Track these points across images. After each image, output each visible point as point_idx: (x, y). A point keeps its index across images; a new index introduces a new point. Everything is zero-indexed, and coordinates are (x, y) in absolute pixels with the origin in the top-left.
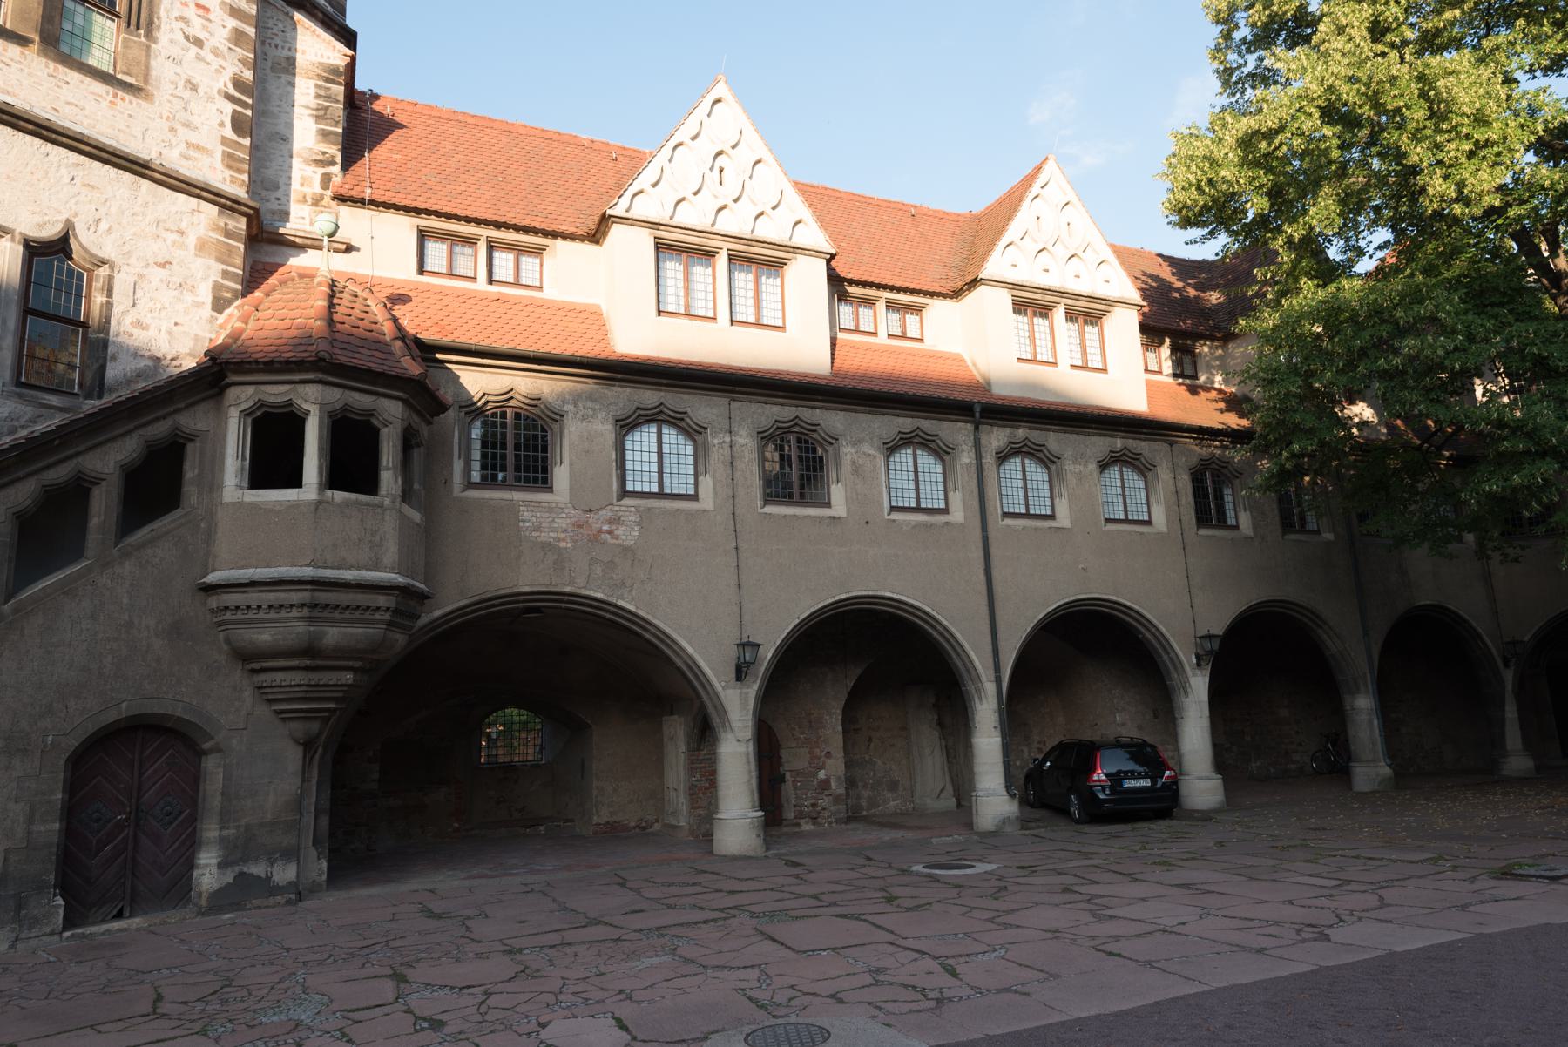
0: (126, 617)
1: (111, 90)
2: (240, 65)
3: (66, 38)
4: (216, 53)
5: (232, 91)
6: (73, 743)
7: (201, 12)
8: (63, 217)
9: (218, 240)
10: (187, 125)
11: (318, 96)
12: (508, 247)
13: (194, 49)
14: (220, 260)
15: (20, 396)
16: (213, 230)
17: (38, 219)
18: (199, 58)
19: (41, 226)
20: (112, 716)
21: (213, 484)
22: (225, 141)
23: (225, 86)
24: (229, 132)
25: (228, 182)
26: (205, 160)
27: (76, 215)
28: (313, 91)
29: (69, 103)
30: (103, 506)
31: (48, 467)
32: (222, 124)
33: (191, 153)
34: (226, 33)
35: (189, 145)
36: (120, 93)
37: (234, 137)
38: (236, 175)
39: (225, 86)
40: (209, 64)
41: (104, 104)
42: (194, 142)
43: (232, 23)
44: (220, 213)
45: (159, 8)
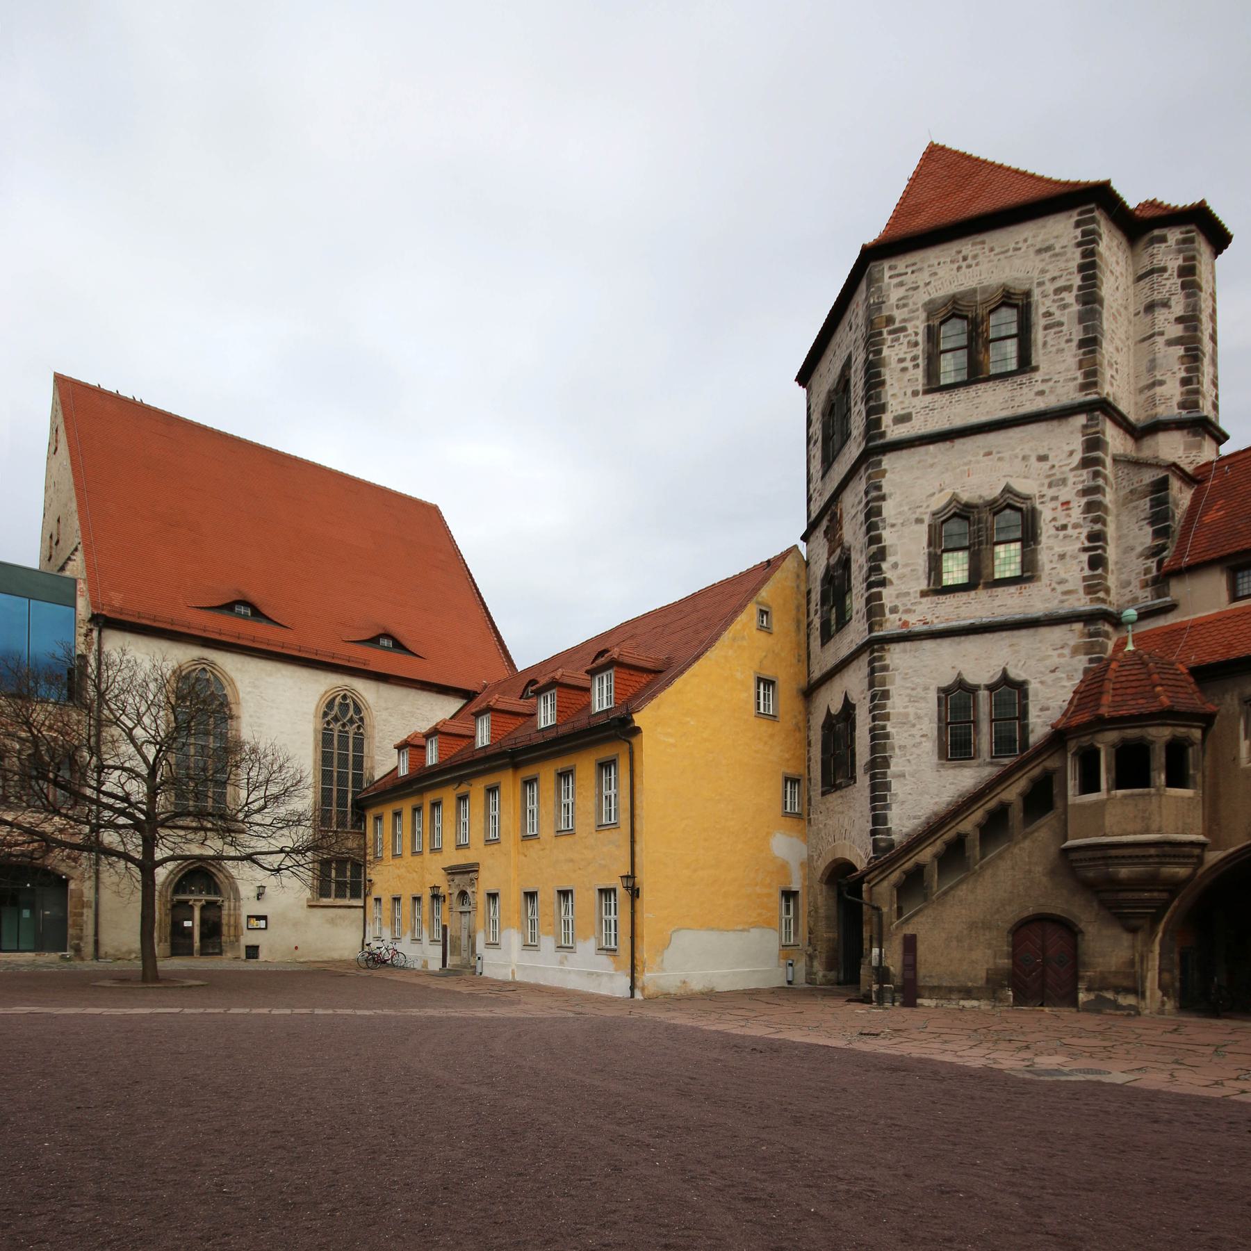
0: (1028, 867)
1: (1019, 586)
2: (1092, 524)
3: (996, 569)
4: (1075, 526)
5: (1087, 544)
6: (1008, 926)
7: (1065, 507)
8: (1001, 668)
9: (1085, 642)
10: (1059, 583)
13: (1062, 533)
14: (1086, 654)
15: (991, 764)
16: (1081, 637)
17: (991, 673)
18: (1065, 537)
19: (992, 677)
20: (1026, 914)
22: (1085, 579)
23: (1083, 544)
24: (1087, 572)
25: (1088, 603)
26: (1075, 596)
27: (1007, 664)
29: (999, 606)
30: (1016, 814)
31: (986, 802)
32: (1082, 570)
33: (1065, 597)
34: (1080, 510)
36: (1023, 586)
37: (1091, 573)
38: (1094, 596)
39: (1083, 544)
40: (1071, 536)
41: (1016, 596)
42: (1066, 589)
43: (1084, 500)
44: (1085, 626)
45: (1040, 521)
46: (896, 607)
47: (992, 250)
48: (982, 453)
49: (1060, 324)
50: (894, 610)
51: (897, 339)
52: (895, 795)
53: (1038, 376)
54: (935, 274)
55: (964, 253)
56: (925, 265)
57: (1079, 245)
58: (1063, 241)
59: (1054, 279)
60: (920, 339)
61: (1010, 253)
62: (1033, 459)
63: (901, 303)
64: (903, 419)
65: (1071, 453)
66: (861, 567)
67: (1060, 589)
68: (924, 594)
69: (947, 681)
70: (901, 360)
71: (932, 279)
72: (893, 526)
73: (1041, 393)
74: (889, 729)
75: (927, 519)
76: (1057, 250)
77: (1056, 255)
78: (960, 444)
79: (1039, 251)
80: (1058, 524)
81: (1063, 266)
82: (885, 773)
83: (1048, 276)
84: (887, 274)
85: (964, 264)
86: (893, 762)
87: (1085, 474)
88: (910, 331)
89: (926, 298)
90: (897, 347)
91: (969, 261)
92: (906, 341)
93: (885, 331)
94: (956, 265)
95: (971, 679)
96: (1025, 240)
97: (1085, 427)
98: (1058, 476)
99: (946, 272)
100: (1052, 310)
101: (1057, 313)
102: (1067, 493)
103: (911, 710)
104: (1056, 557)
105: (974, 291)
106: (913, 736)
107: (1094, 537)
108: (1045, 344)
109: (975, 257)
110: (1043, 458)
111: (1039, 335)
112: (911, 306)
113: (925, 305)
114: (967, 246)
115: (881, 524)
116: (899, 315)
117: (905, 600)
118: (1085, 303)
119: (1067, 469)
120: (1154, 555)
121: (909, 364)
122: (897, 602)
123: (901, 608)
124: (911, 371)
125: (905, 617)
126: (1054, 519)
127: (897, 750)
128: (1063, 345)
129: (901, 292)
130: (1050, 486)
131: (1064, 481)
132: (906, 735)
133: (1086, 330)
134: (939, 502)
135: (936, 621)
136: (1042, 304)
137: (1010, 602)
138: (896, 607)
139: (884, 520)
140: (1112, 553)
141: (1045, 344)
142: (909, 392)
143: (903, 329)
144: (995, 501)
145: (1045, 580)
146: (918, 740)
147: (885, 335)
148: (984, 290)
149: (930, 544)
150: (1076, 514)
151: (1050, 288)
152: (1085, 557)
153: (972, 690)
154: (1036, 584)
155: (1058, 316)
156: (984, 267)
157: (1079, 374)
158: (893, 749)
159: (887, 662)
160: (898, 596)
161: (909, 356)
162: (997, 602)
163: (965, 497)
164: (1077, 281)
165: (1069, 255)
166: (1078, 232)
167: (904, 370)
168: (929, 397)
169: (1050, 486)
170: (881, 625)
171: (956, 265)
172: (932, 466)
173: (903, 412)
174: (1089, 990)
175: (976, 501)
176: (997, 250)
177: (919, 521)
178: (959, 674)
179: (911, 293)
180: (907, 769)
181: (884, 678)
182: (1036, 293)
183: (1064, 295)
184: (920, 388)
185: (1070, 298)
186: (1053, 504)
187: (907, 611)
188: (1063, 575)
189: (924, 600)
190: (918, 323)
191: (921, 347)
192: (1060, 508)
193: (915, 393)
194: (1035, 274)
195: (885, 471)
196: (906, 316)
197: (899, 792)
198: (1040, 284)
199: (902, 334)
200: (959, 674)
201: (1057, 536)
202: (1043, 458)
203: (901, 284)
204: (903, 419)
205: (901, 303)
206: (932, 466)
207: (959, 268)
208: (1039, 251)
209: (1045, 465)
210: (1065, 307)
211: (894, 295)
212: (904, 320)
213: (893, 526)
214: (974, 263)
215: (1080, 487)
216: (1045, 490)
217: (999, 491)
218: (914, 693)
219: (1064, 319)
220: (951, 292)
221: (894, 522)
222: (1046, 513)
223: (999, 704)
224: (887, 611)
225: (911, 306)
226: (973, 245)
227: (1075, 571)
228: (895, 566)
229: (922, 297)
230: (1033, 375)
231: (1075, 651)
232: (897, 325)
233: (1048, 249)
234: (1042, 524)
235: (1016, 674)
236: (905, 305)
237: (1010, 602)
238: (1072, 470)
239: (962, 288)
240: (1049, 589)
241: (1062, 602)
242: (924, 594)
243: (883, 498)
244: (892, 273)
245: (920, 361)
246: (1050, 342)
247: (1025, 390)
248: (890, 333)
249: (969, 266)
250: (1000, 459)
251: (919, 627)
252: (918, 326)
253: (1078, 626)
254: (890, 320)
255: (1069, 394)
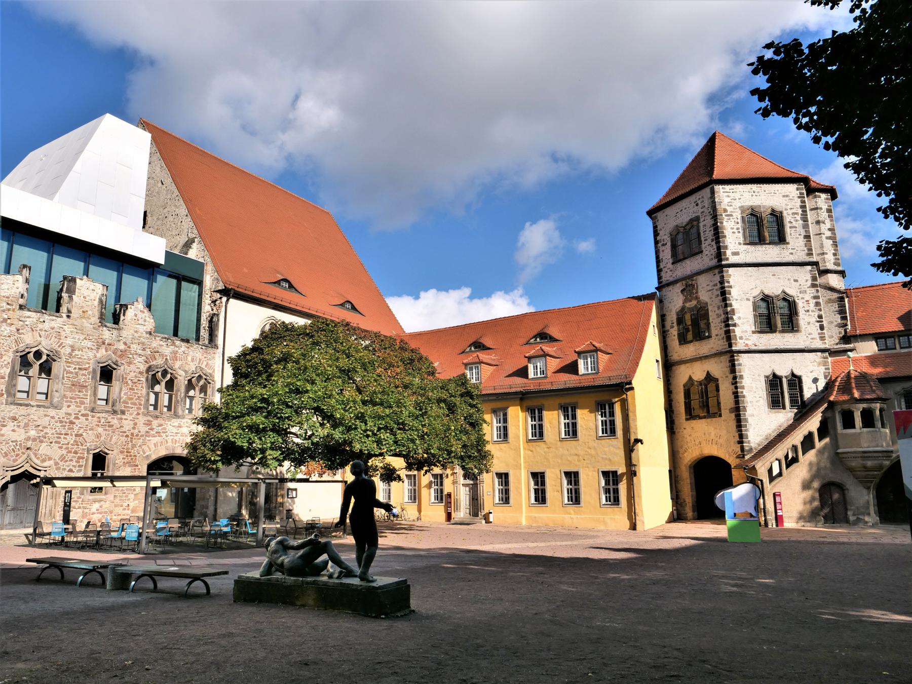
5: (818, 320)
11: (839, 307)
12: (902, 336)
13: (808, 313)
14: (824, 366)
18: (809, 315)
21: (835, 428)
22: (819, 334)
28: (837, 306)
33: (812, 341)
34: (813, 305)
35: (812, 339)
43: (815, 301)
46: (742, 337)
47: (765, 191)
48: (771, 274)
49: (796, 227)
50: (741, 338)
51: (729, 219)
52: (750, 425)
53: (789, 246)
54: (742, 195)
55: (753, 190)
56: (738, 191)
57: (799, 197)
58: (793, 195)
59: (791, 209)
60: (740, 221)
61: (772, 194)
62: (792, 281)
63: (729, 204)
64: (736, 254)
65: (807, 281)
66: (718, 316)
67: (810, 337)
68: (754, 332)
69: (769, 372)
70: (732, 228)
71: (741, 197)
72: (737, 300)
73: (792, 254)
74: (744, 393)
75: (752, 299)
76: (791, 198)
77: (791, 199)
78: (761, 268)
79: (784, 196)
80: (806, 309)
81: (794, 204)
82: (745, 414)
83: (788, 207)
84: (722, 190)
85: (754, 194)
86: (747, 409)
87: (813, 290)
88: (735, 217)
89: (740, 205)
90: (729, 222)
91: (756, 194)
92: (733, 220)
93: (724, 214)
94: (751, 194)
95: (778, 373)
96: (778, 191)
97: (811, 271)
98: (803, 289)
99: (747, 196)
100: (792, 221)
101: (794, 223)
102: (808, 297)
103: (754, 385)
104: (806, 324)
105: (760, 206)
106: (755, 397)
107: (820, 317)
108: (791, 234)
109: (758, 192)
110: (796, 281)
111: (788, 230)
112: (734, 207)
113: (739, 207)
114: (754, 187)
115: (731, 299)
116: (729, 209)
117: (746, 334)
118: (804, 221)
119: (806, 287)
120: (842, 327)
121: (735, 230)
122: (742, 335)
123: (744, 338)
124: (737, 234)
125: (747, 342)
126: (804, 307)
127: (749, 404)
128: (798, 236)
129: (728, 200)
130: (800, 292)
131: (805, 291)
132: (752, 396)
133: (806, 231)
134: (756, 292)
135: (760, 345)
136: (788, 219)
137: (790, 340)
138: (742, 337)
139: (732, 297)
140: (825, 323)
141: (791, 234)
142: (737, 243)
143: (732, 215)
144: (779, 295)
145: (803, 332)
146: (758, 399)
147: (724, 216)
148: (764, 207)
149: (754, 311)
150: (812, 306)
151: (790, 212)
152: (818, 324)
153: (780, 378)
154: (800, 334)
155: (794, 224)
156: (762, 197)
157: (805, 249)
158: (747, 403)
159: (741, 362)
160: (742, 332)
161: (735, 227)
162: (785, 340)
163: (766, 292)
164: (800, 211)
165: (796, 200)
166: (798, 192)
167: (734, 233)
168: (746, 247)
169: (800, 292)
170: (736, 344)
171: (751, 194)
172: (751, 276)
173: (735, 251)
174: (854, 515)
175: (771, 294)
176: (767, 192)
177: (748, 299)
178: (773, 370)
179: (733, 201)
180: (755, 413)
181: (740, 369)
182: (785, 214)
183: (796, 216)
184: (742, 242)
185: (798, 217)
186: (803, 301)
187: (747, 339)
188: (810, 331)
189: (754, 335)
190: (737, 214)
191: (740, 224)
192: (805, 303)
193: (740, 244)
194: (784, 205)
195: (730, 275)
196: (733, 210)
197: (752, 423)
198: (786, 209)
199: (731, 218)
200: (773, 370)
201: (806, 315)
202: (796, 281)
203: (728, 196)
204: (736, 254)
205: (729, 204)
206: (751, 276)
207: (752, 195)
208: (784, 196)
209: (797, 284)
210: (797, 221)
211: (726, 200)
212: (732, 212)
213: (737, 300)
214: (758, 194)
215: (812, 295)
216: (799, 295)
217: (780, 292)
218: (754, 377)
219: (797, 226)
220: (751, 204)
221: (736, 298)
222: (801, 305)
223: (791, 384)
224: (738, 338)
225: (734, 207)
226: (757, 187)
227: (815, 330)
228: (739, 318)
229: (738, 204)
230: (787, 245)
231: (819, 364)
232: (728, 213)
233: (787, 196)
234: (799, 308)
235: (797, 372)
236: (731, 205)
237: (790, 340)
238: (808, 287)
239: (754, 204)
240: (805, 337)
241: (811, 342)
242: (754, 332)
243: (731, 287)
244: (724, 190)
245: (740, 230)
246: (793, 234)
247: (785, 251)
248: (726, 216)
249: (757, 196)
250: (779, 278)
251: (753, 348)
252: (738, 215)
253: (819, 354)
254: (725, 211)
255: (801, 256)
